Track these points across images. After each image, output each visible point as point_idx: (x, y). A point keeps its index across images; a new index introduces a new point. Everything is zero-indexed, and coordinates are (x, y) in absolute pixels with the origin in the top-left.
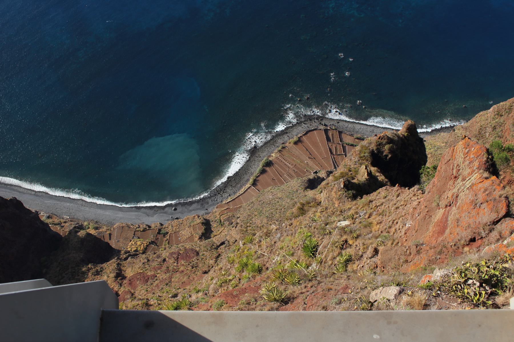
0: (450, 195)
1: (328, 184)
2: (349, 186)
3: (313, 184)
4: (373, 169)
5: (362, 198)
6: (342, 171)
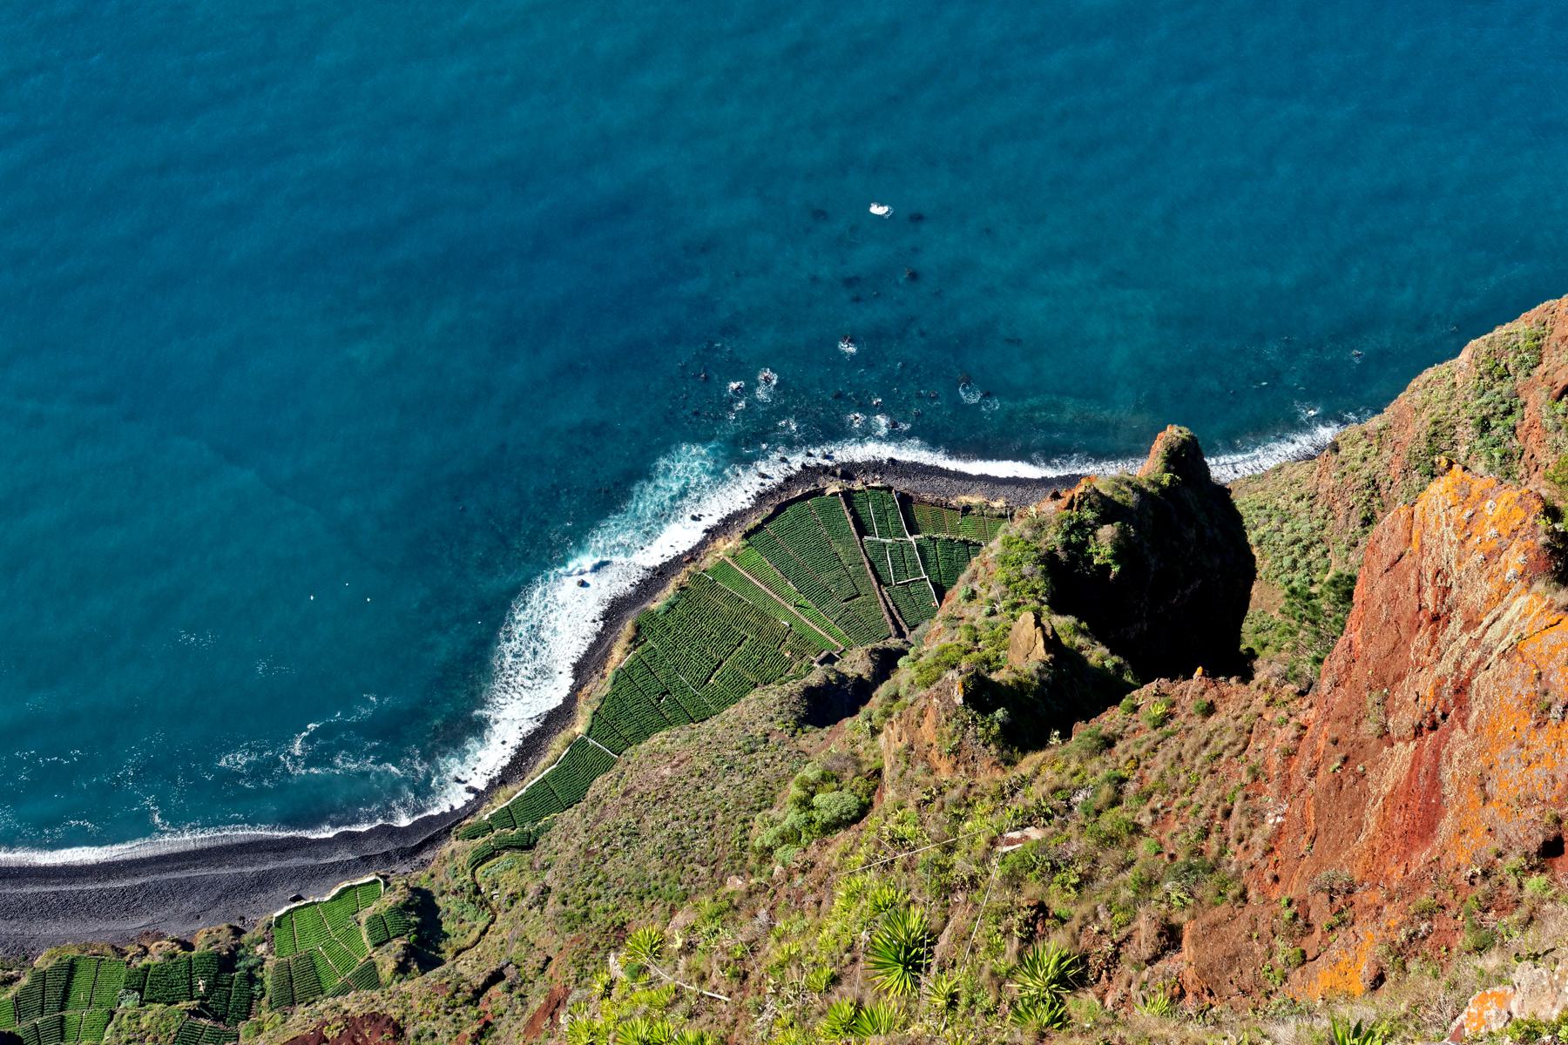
1: (896, 697)
2: (982, 694)
6: (945, 641)
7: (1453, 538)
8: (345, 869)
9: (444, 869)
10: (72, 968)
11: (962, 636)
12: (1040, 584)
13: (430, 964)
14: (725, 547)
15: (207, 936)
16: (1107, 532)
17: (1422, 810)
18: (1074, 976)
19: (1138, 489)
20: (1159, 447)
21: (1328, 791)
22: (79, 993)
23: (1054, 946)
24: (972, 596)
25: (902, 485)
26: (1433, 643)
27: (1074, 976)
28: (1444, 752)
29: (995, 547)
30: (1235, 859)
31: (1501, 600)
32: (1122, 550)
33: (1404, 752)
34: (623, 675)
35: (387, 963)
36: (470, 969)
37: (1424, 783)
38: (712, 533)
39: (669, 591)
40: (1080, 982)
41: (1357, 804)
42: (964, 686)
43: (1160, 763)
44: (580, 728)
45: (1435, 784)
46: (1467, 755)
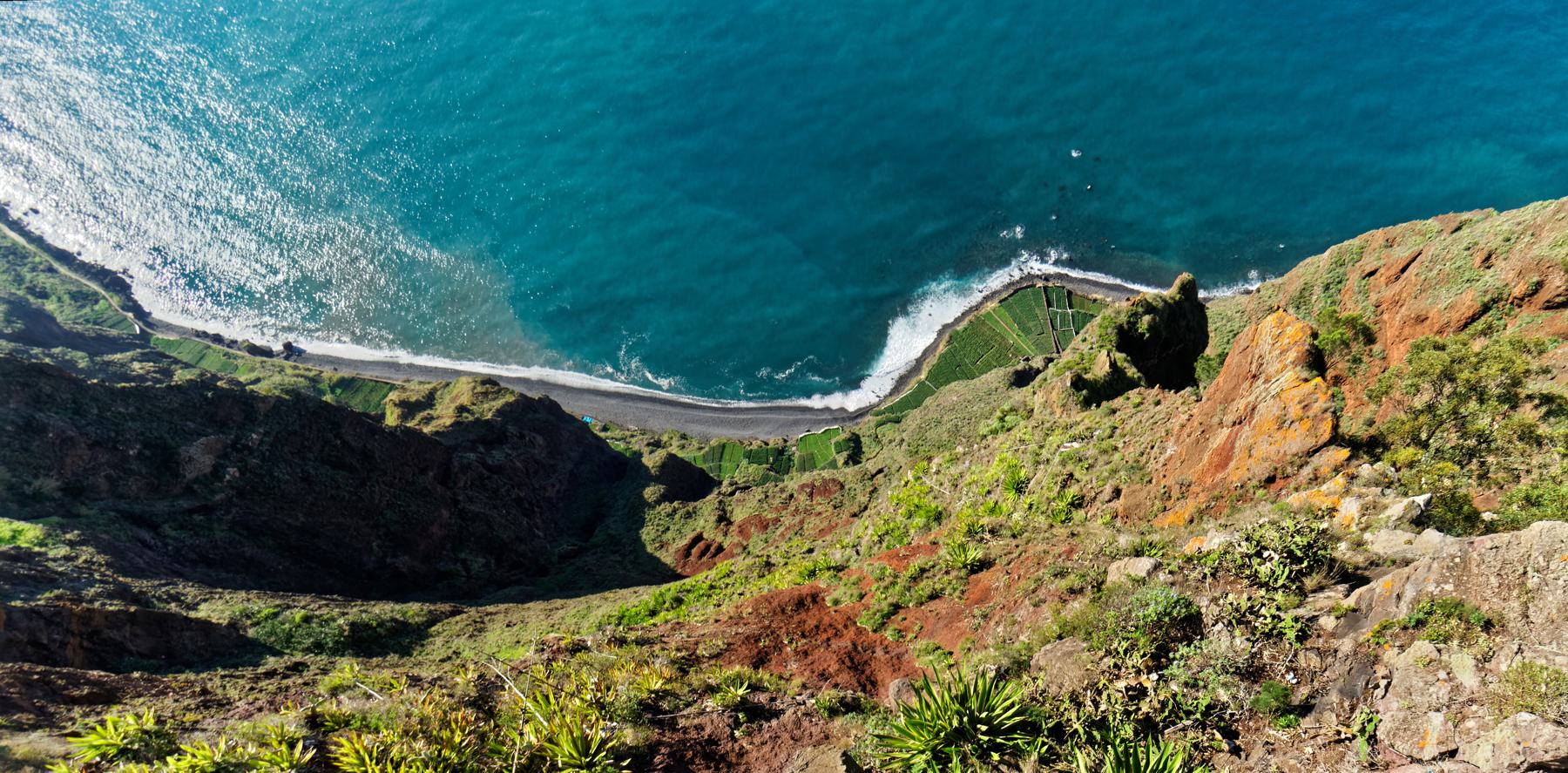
0: (1242, 407)
2: (1078, 383)
3: (1023, 378)
4: (1120, 357)
5: (1098, 406)
6: (1070, 358)
8: (827, 422)
9: (865, 427)
10: (724, 446)
11: (1077, 357)
12: (1114, 338)
13: (856, 462)
14: (991, 305)
15: (774, 441)
16: (1147, 318)
17: (1224, 457)
18: (1078, 503)
19: (1165, 301)
20: (1177, 282)
22: (726, 456)
23: (1073, 491)
24: (1084, 340)
25: (1069, 286)
27: (1078, 503)
29: (1098, 320)
30: (1151, 466)
32: (1151, 328)
33: (1226, 431)
34: (943, 356)
35: (841, 460)
36: (871, 466)
38: (986, 299)
39: (965, 323)
40: (1080, 506)
43: (1132, 422)
44: (923, 377)
45: (1233, 447)
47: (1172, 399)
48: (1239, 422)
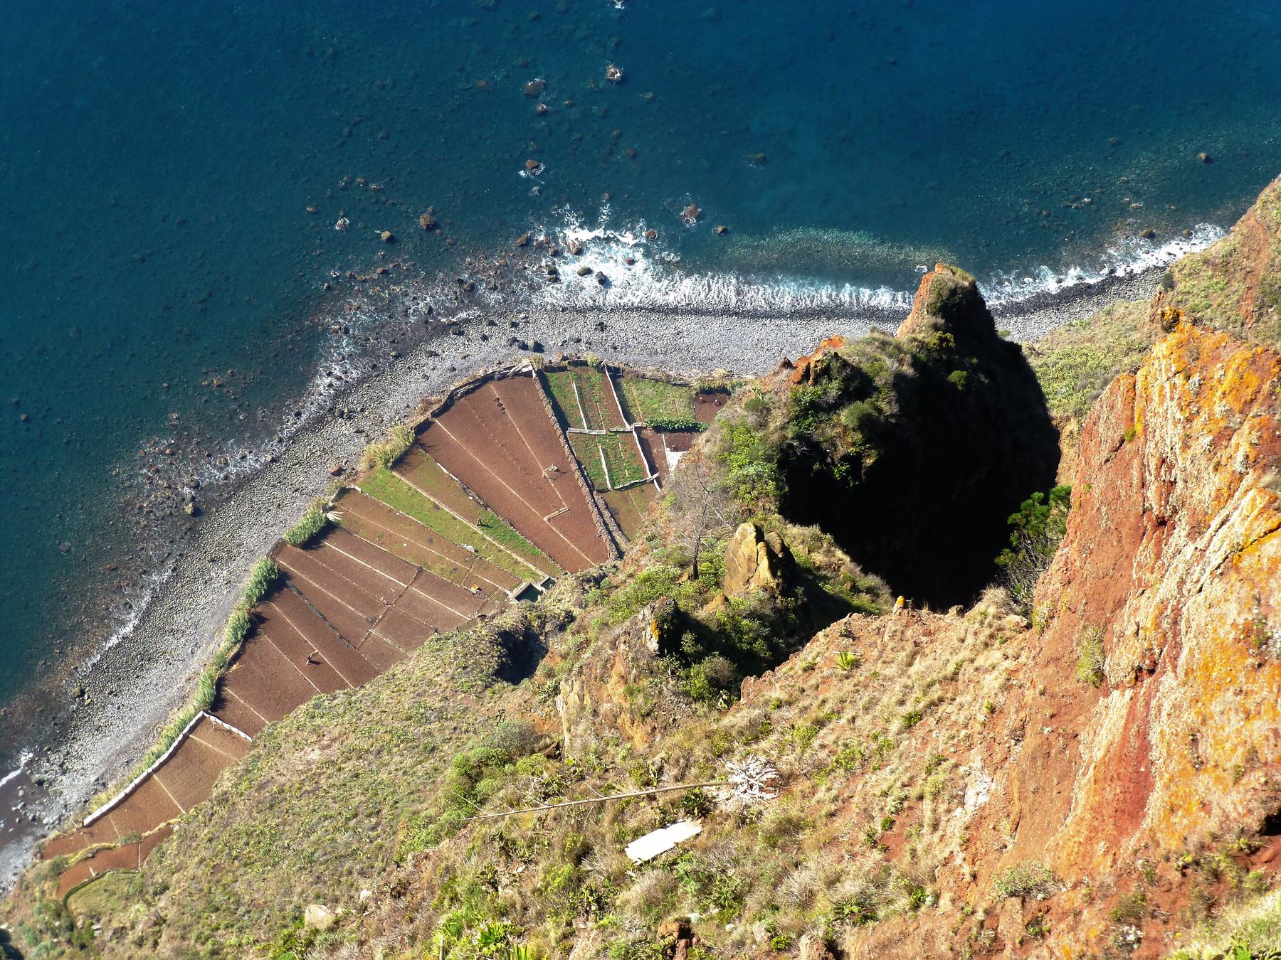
7: (1178, 415)
21: (1034, 759)
26: (1158, 556)
28: (1154, 703)
31: (1231, 496)
37: (1135, 742)
41: (1067, 775)
42: (659, 627)
46: (1176, 707)
47: (953, 627)
48: (1145, 671)
